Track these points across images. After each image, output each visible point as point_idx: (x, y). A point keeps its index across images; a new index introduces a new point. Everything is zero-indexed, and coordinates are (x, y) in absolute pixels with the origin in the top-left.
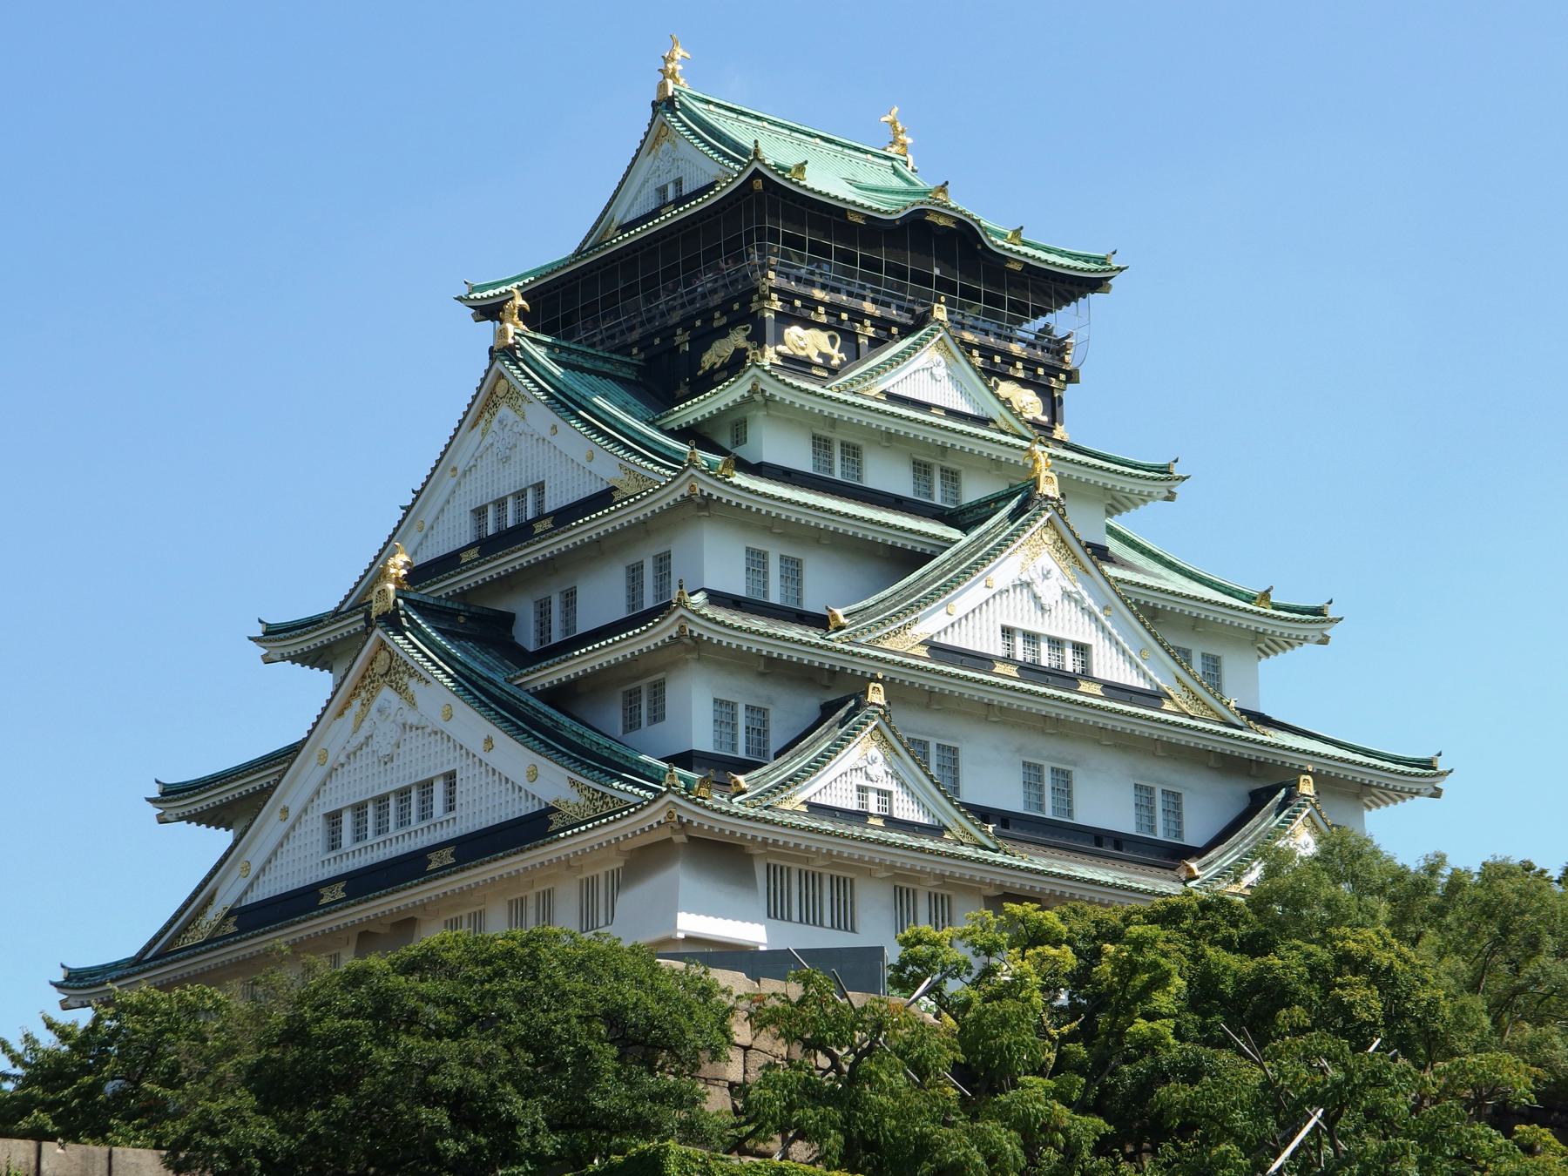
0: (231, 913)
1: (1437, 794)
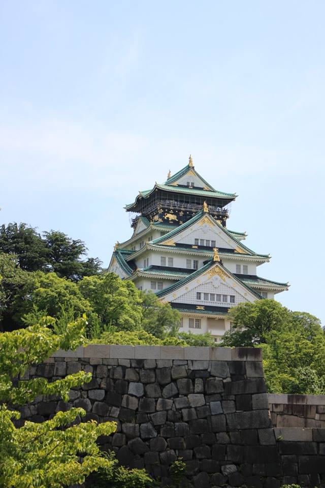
0: (169, 303)
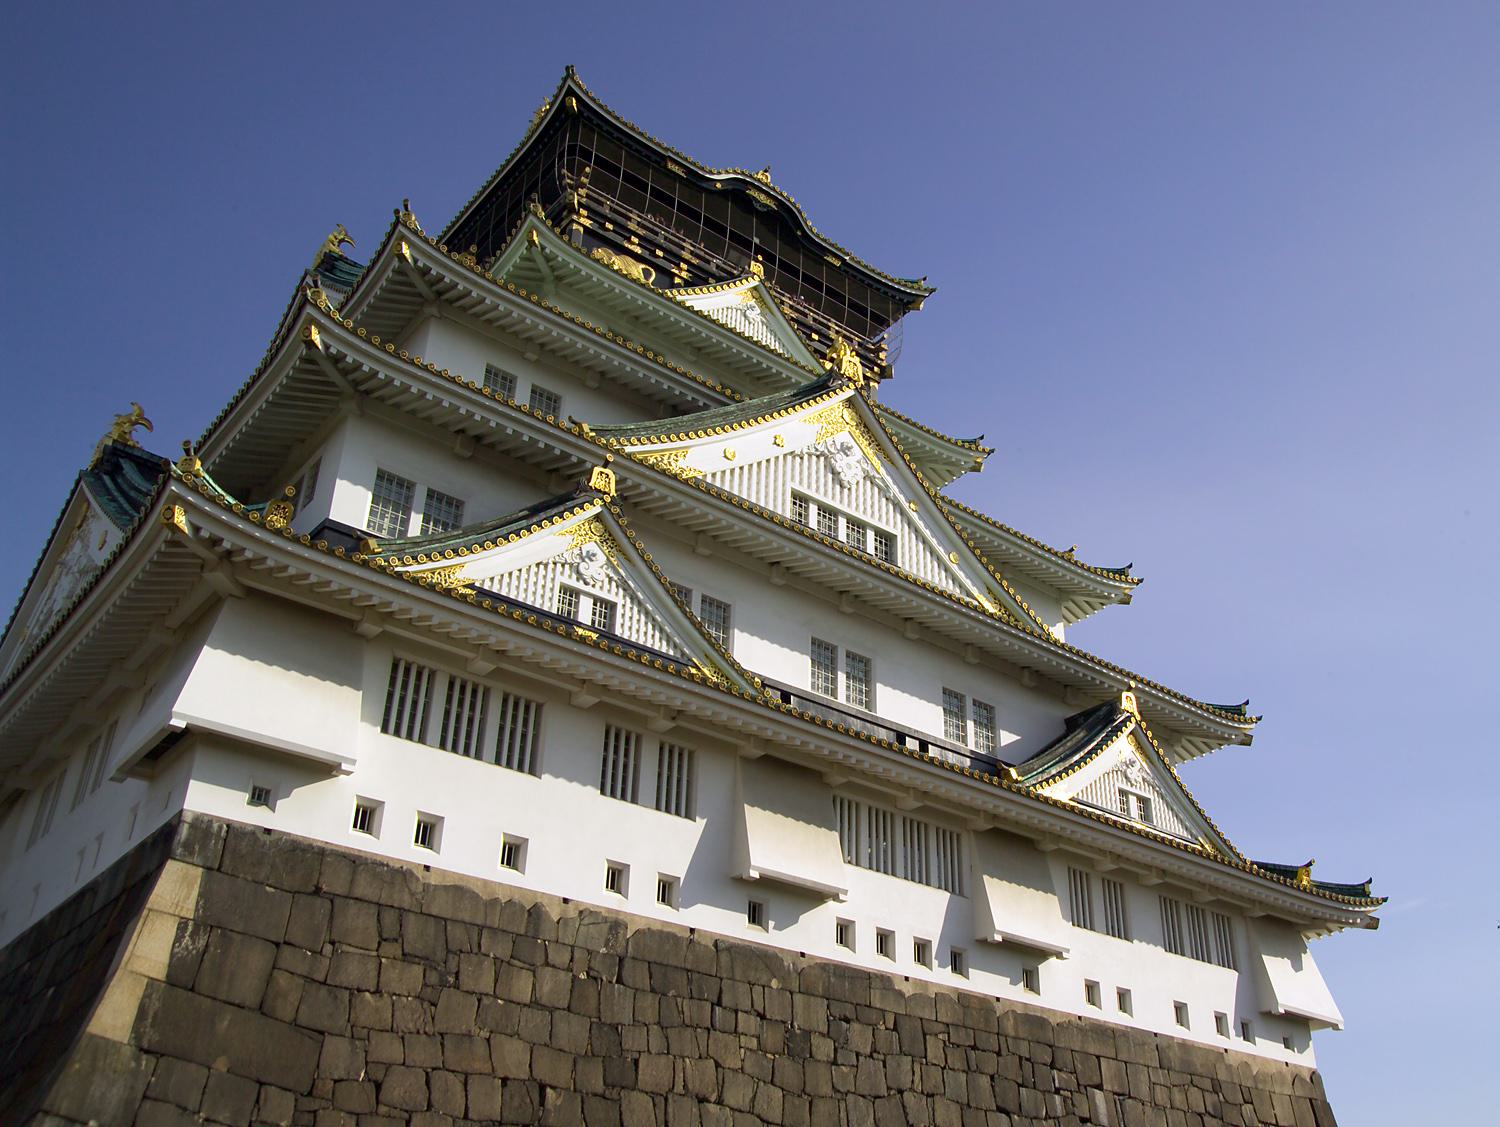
1: (1247, 741)
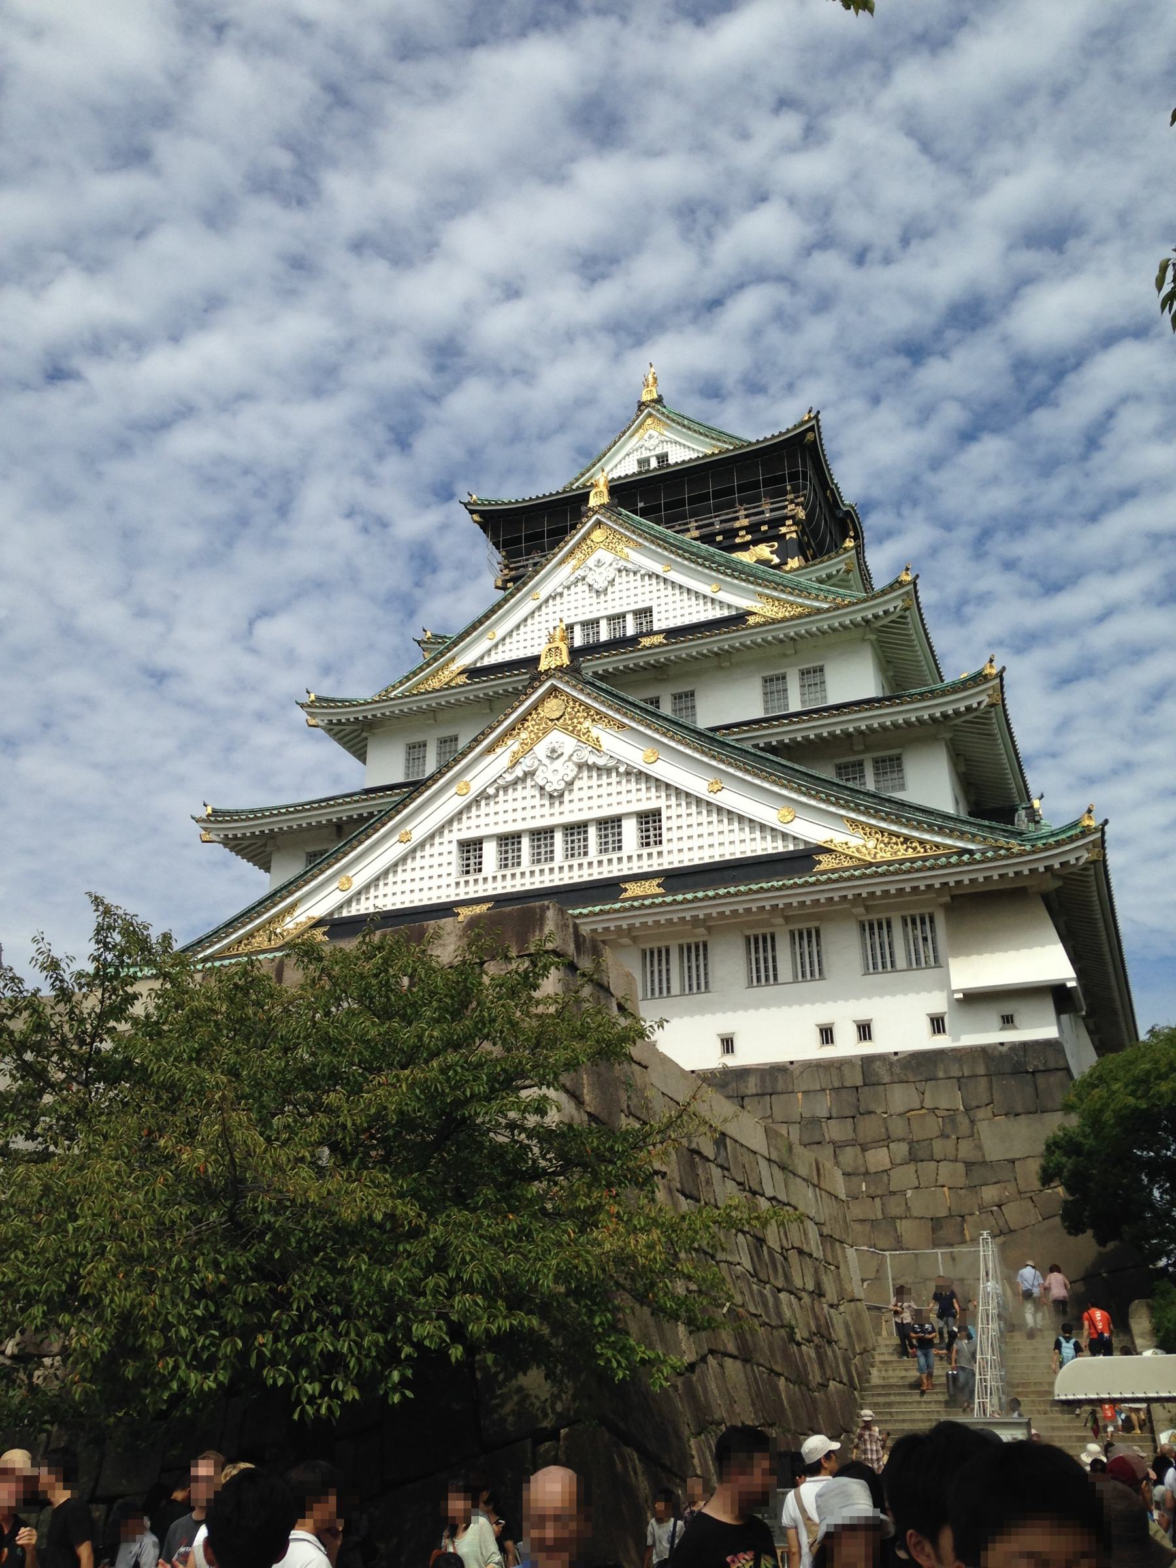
0: (319, 923)
